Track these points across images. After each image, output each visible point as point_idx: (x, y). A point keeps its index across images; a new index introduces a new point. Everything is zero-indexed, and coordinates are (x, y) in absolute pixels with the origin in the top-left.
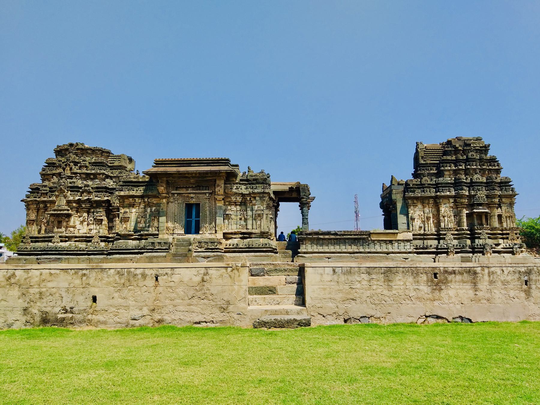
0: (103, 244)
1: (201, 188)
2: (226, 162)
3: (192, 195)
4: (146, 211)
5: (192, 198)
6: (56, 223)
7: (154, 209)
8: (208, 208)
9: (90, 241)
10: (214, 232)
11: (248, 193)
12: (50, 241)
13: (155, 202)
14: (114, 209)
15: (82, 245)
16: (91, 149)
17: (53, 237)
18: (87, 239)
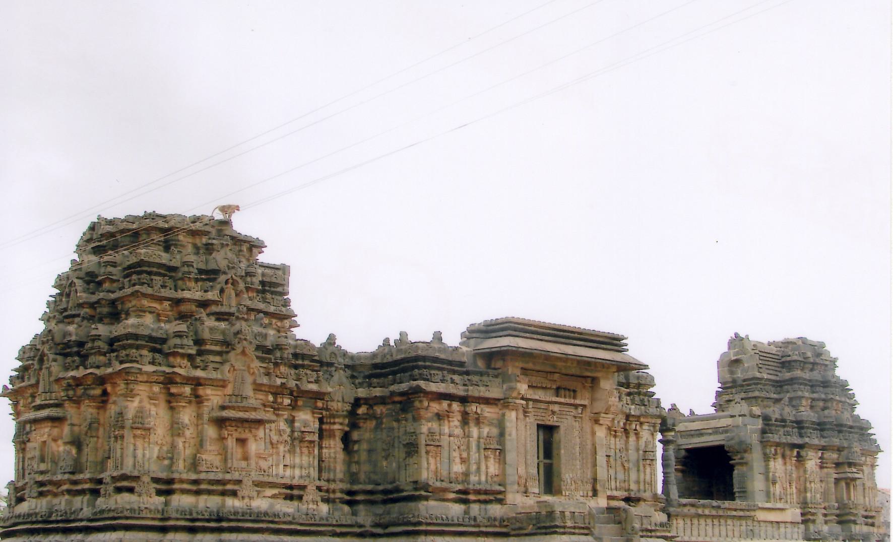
0: (324, 508)
1: (562, 392)
2: (614, 342)
3: (556, 408)
4: (468, 436)
5: (553, 413)
6: (231, 443)
7: (486, 430)
8: (578, 440)
9: (300, 498)
10: (590, 494)
11: (638, 413)
12: (234, 494)
13: (486, 414)
14: (334, 416)
15: (286, 508)
16: (249, 242)
17: (239, 482)
18: (293, 492)
